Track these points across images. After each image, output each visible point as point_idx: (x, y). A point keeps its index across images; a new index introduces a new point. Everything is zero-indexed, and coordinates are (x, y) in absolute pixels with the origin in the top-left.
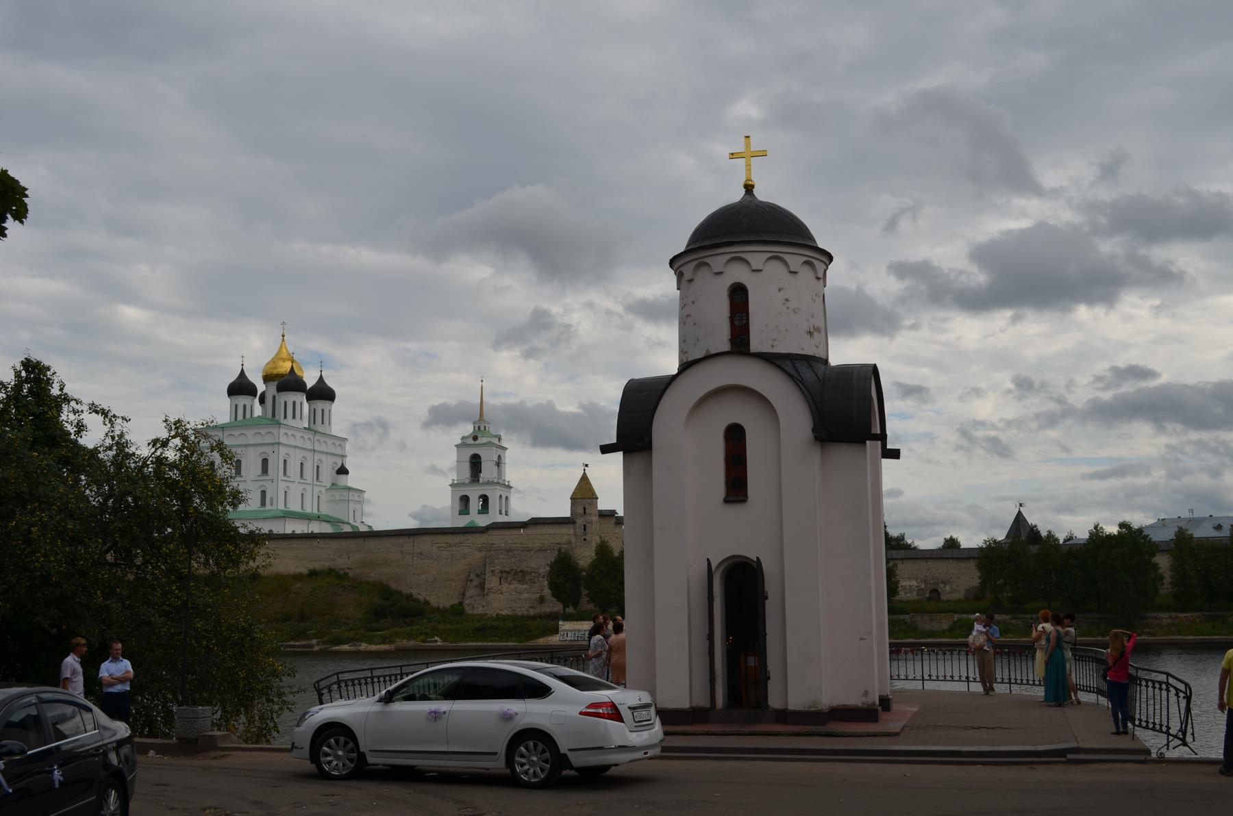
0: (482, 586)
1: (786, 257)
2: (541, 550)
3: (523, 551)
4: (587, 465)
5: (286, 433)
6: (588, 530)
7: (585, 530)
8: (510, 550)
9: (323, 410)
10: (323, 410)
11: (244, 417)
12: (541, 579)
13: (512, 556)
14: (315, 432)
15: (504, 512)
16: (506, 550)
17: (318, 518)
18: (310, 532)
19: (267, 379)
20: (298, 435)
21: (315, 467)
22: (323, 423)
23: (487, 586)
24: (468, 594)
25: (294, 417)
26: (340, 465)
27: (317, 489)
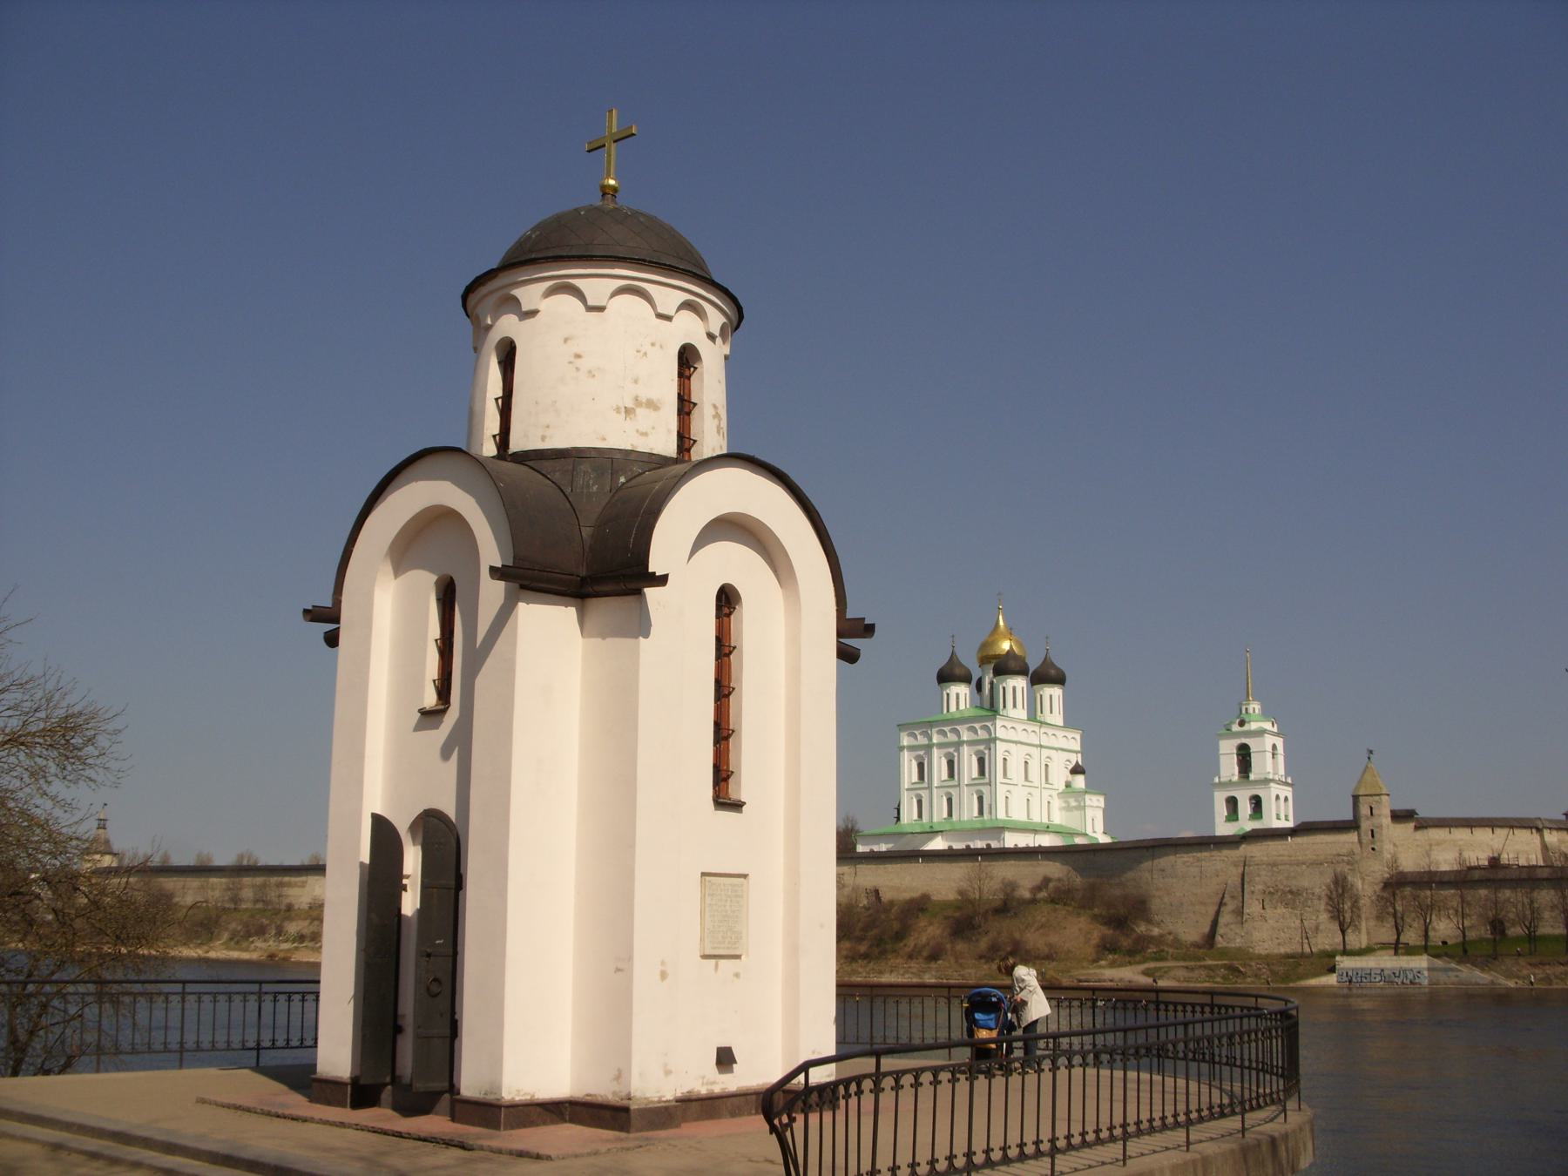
0: (1240, 912)
1: (577, 282)
2: (1317, 864)
3: (1291, 864)
4: (1371, 752)
5: (1004, 726)
6: (1375, 835)
7: (1373, 836)
8: (1274, 864)
9: (1051, 696)
10: (1051, 696)
11: (958, 708)
12: (1316, 902)
13: (1278, 872)
14: (1041, 722)
15: (1282, 817)
16: (1269, 864)
17: (1047, 829)
18: (1037, 845)
19: (984, 661)
20: (1020, 727)
21: (1043, 767)
22: (1051, 712)
23: (1246, 910)
24: (1222, 920)
25: (1015, 706)
26: (1074, 763)
27: (1046, 793)
